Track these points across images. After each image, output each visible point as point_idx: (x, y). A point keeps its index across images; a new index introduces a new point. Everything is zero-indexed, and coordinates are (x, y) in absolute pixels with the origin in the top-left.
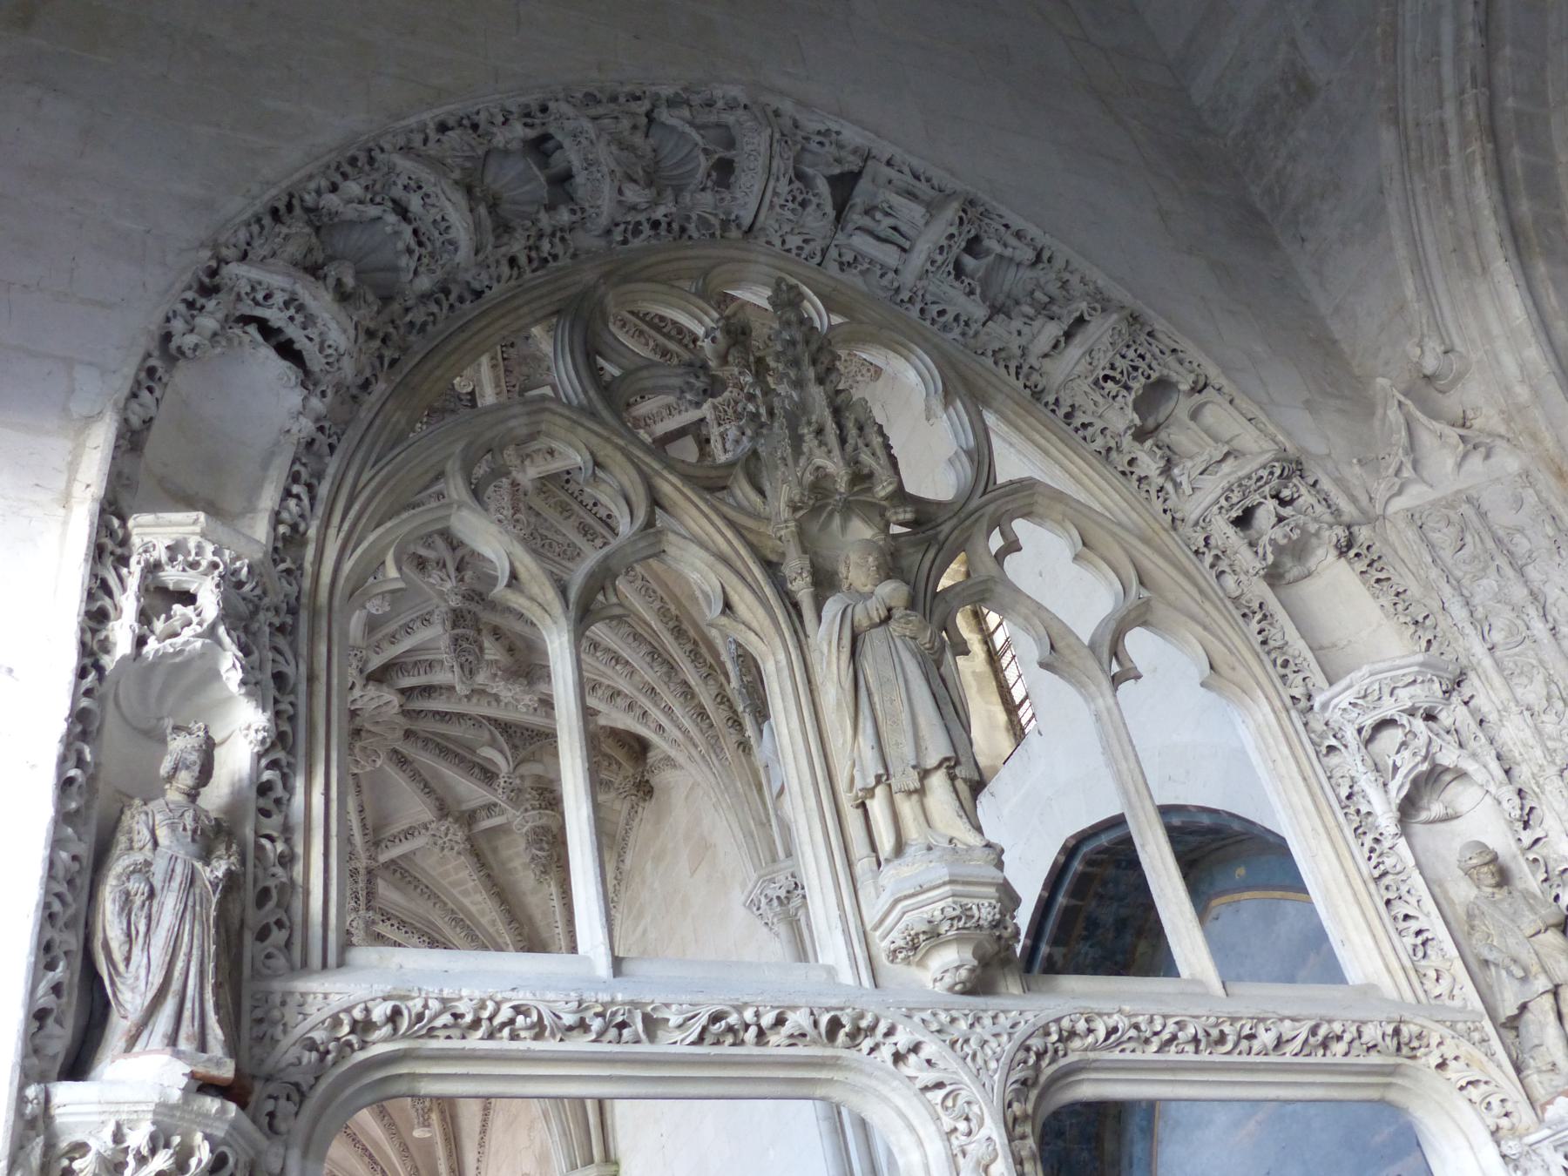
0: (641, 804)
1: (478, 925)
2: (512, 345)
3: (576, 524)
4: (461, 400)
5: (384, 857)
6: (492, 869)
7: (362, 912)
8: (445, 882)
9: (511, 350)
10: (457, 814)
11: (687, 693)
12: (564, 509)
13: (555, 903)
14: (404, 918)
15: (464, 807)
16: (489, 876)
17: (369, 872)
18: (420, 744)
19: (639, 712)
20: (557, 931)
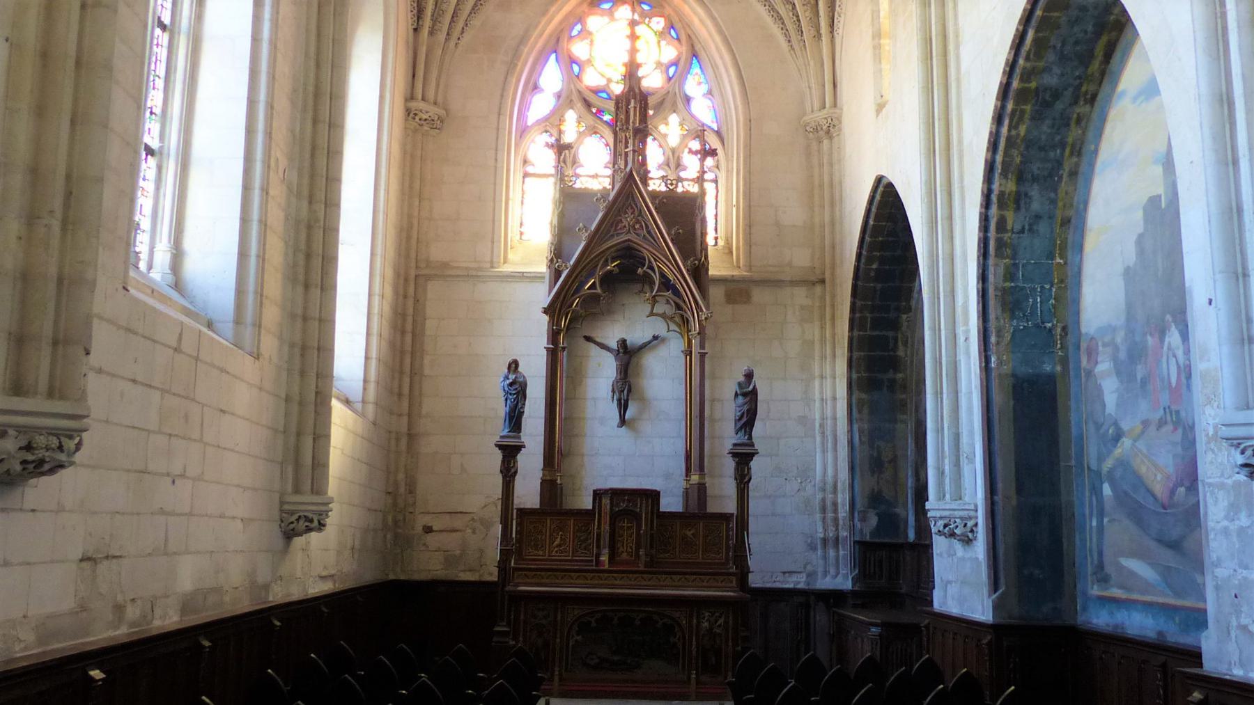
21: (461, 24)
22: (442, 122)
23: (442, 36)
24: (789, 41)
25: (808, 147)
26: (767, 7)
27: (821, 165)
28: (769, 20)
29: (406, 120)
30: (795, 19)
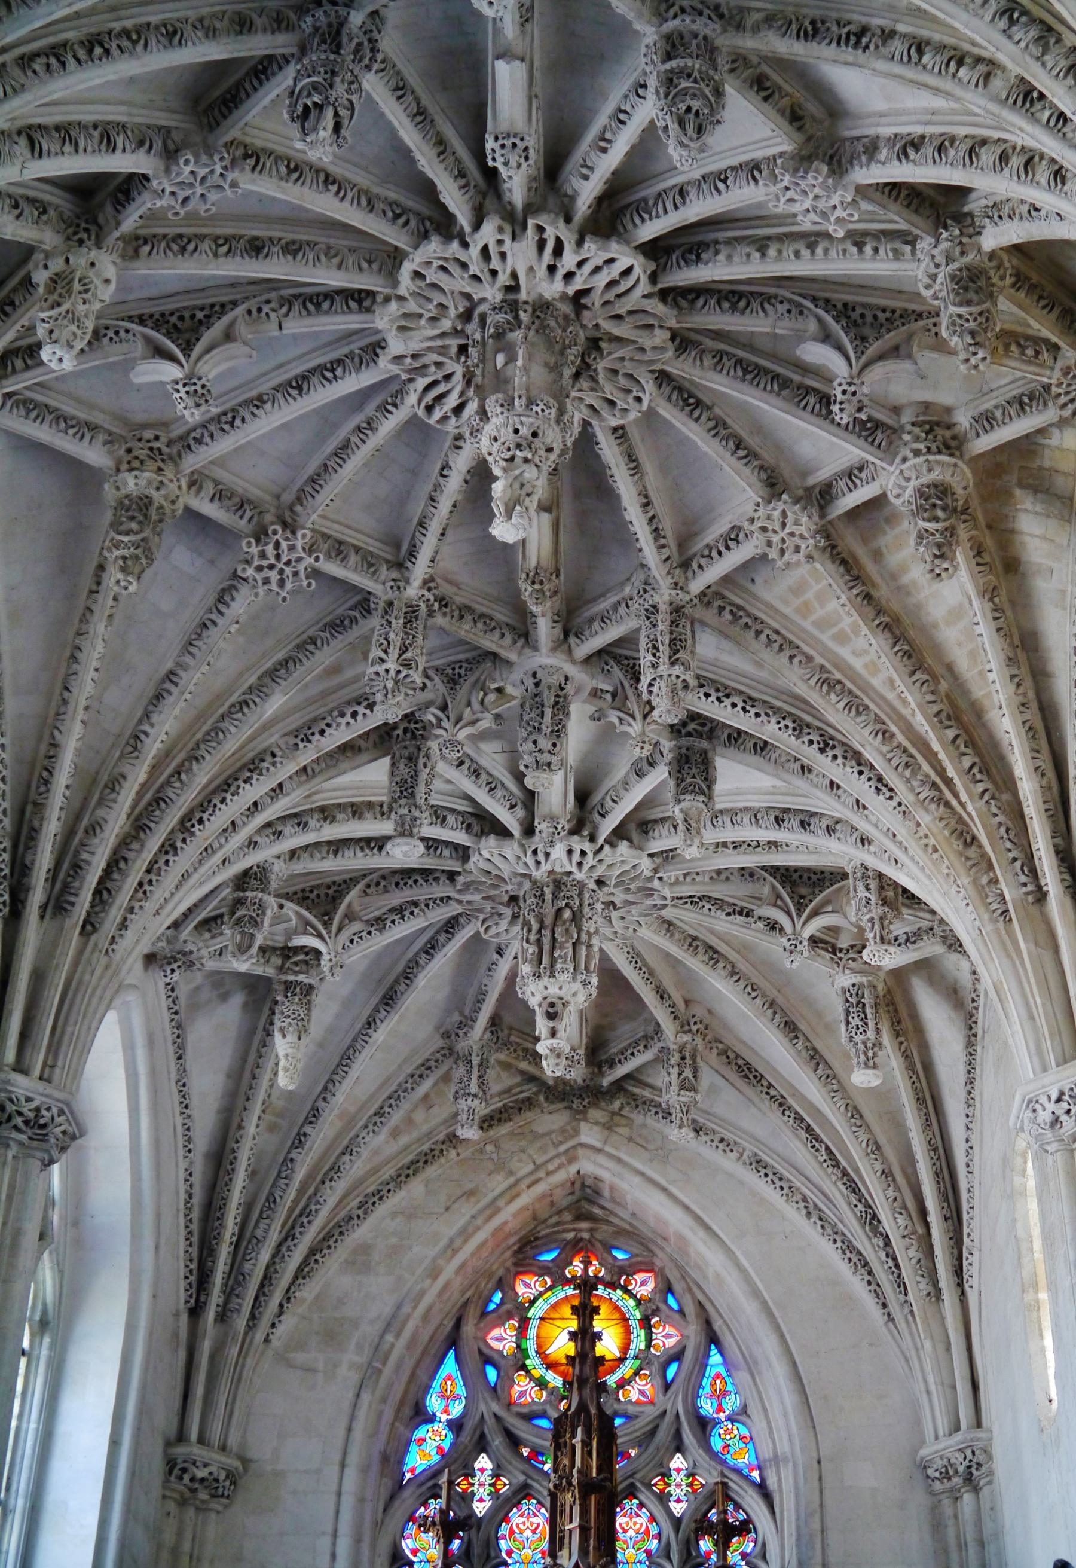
1: (866, 688)
5: (696, 586)
6: (874, 585)
7: (663, 669)
8: (807, 624)
10: (801, 492)
13: (981, 629)
14: (754, 694)
15: (811, 481)
16: (868, 597)
17: (677, 610)
18: (708, 361)
19: (1016, 161)
20: (992, 676)
21: (277, 1297)
22: (234, 1483)
23: (240, 1323)
24: (884, 1306)
25: (935, 1511)
26: (839, 1244)
27: (962, 1546)
28: (844, 1269)
29: (166, 1481)
30: (891, 1263)
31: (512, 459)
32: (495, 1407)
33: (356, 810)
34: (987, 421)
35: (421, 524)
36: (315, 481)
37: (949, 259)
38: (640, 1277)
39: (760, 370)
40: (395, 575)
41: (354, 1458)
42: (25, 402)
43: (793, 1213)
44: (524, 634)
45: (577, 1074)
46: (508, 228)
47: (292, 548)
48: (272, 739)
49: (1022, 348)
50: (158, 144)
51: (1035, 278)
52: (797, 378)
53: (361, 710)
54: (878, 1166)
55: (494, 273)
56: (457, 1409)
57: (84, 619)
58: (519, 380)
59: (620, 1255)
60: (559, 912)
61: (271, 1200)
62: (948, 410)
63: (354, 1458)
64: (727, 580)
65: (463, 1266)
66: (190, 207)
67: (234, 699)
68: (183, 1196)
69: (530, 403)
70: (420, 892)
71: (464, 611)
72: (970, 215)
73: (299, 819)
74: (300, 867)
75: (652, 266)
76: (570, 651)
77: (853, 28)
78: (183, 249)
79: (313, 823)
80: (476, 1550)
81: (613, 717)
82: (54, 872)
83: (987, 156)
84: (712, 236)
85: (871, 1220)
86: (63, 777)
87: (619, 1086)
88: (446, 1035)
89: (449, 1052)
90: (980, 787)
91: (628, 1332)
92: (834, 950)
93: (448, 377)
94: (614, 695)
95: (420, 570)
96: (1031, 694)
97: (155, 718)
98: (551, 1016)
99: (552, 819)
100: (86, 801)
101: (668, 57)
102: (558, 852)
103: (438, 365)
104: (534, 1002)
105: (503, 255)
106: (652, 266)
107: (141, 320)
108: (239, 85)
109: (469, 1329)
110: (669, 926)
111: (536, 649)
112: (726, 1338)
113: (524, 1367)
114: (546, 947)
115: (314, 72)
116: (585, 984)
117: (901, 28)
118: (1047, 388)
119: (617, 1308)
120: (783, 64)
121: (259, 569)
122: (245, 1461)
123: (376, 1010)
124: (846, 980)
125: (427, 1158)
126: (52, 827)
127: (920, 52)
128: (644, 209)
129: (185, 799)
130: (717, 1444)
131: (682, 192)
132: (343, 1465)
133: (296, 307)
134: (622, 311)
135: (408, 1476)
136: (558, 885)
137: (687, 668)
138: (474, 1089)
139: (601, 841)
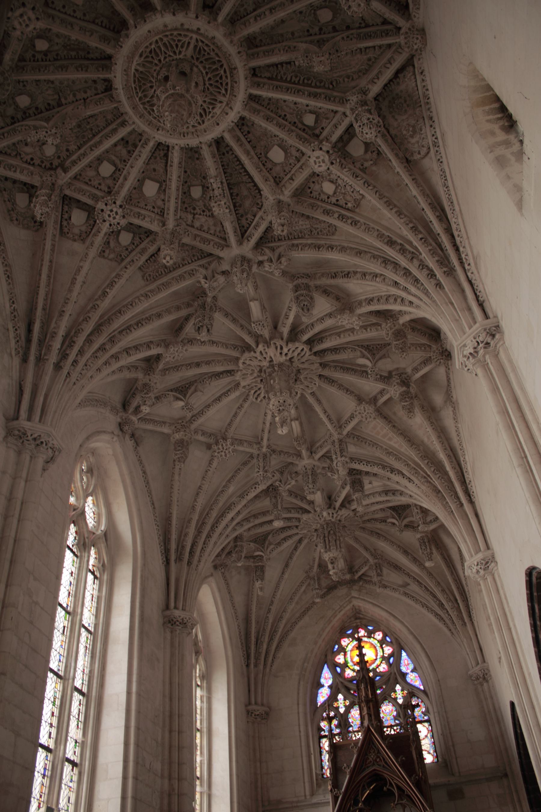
0: (449, 362)
2: (249, 132)
3: (322, 211)
4: (241, 173)
5: (345, 433)
7: (339, 459)
8: (379, 437)
9: (250, 135)
11: (407, 273)
12: (313, 206)
15: (371, 396)
16: (394, 426)
17: (340, 441)
18: (332, 369)
19: (399, 300)
23: (261, 667)
31: (279, 410)
32: (341, 680)
33: (264, 514)
34: (416, 370)
35: (263, 431)
36: (230, 425)
37: (391, 329)
38: (377, 634)
39: (348, 369)
40: (258, 446)
41: (301, 702)
42: (145, 419)
43: (418, 607)
44: (299, 455)
45: (348, 577)
46: (266, 345)
47: (226, 445)
48: (234, 499)
49: (421, 348)
50: (163, 344)
51: (419, 327)
52: (359, 369)
53: (257, 486)
54: (440, 589)
55: (265, 358)
56: (330, 682)
57: (172, 477)
58: (277, 387)
59: (370, 628)
60: (329, 532)
61: (264, 630)
62: (405, 369)
63: (301, 702)
64: (354, 429)
65: (324, 639)
66: (175, 359)
67: (220, 490)
68: (238, 633)
69: (281, 393)
70: (290, 533)
71: (281, 452)
72: (395, 315)
73: (247, 520)
74: (252, 532)
75: (309, 347)
76: (313, 458)
77: (346, 273)
78: (178, 370)
79: (252, 520)
80: (342, 724)
81: (329, 474)
82: (177, 550)
83: (392, 300)
84: (324, 335)
85: (441, 605)
86: (174, 522)
87: (360, 578)
88: (307, 572)
89: (308, 577)
90: (438, 476)
91: (376, 650)
92: (413, 527)
93: (259, 389)
94: (329, 468)
95: (265, 443)
96: (447, 446)
97: (198, 500)
98: (332, 563)
99: (319, 506)
100: (183, 527)
101: (296, 291)
102: (325, 514)
103: (256, 386)
104: (327, 559)
105: (266, 353)
106: (309, 347)
107: (172, 391)
108: (182, 324)
109: (329, 657)
110: (363, 529)
111: (303, 459)
112: (406, 647)
113: (347, 666)
114: (327, 543)
115: (199, 317)
116: (340, 551)
117: (359, 270)
118: (430, 357)
119: (372, 644)
120: (331, 286)
121: (218, 453)
122: (270, 708)
123: (284, 569)
124: (419, 536)
125: (308, 609)
126: (174, 537)
127: (365, 276)
128: (303, 332)
129: (210, 522)
130: (408, 680)
131: (312, 325)
132: (298, 704)
133: (213, 378)
134: (304, 361)
135: (319, 704)
136: (327, 524)
137: (346, 457)
138: (317, 587)
139: (337, 509)
